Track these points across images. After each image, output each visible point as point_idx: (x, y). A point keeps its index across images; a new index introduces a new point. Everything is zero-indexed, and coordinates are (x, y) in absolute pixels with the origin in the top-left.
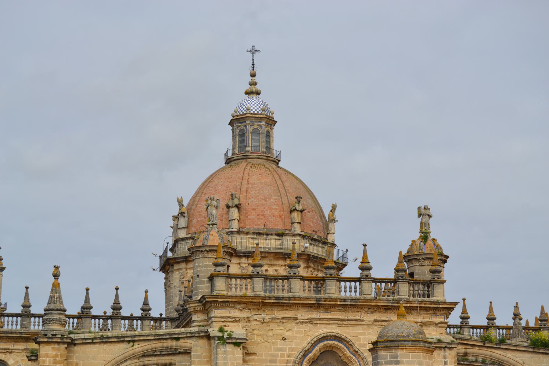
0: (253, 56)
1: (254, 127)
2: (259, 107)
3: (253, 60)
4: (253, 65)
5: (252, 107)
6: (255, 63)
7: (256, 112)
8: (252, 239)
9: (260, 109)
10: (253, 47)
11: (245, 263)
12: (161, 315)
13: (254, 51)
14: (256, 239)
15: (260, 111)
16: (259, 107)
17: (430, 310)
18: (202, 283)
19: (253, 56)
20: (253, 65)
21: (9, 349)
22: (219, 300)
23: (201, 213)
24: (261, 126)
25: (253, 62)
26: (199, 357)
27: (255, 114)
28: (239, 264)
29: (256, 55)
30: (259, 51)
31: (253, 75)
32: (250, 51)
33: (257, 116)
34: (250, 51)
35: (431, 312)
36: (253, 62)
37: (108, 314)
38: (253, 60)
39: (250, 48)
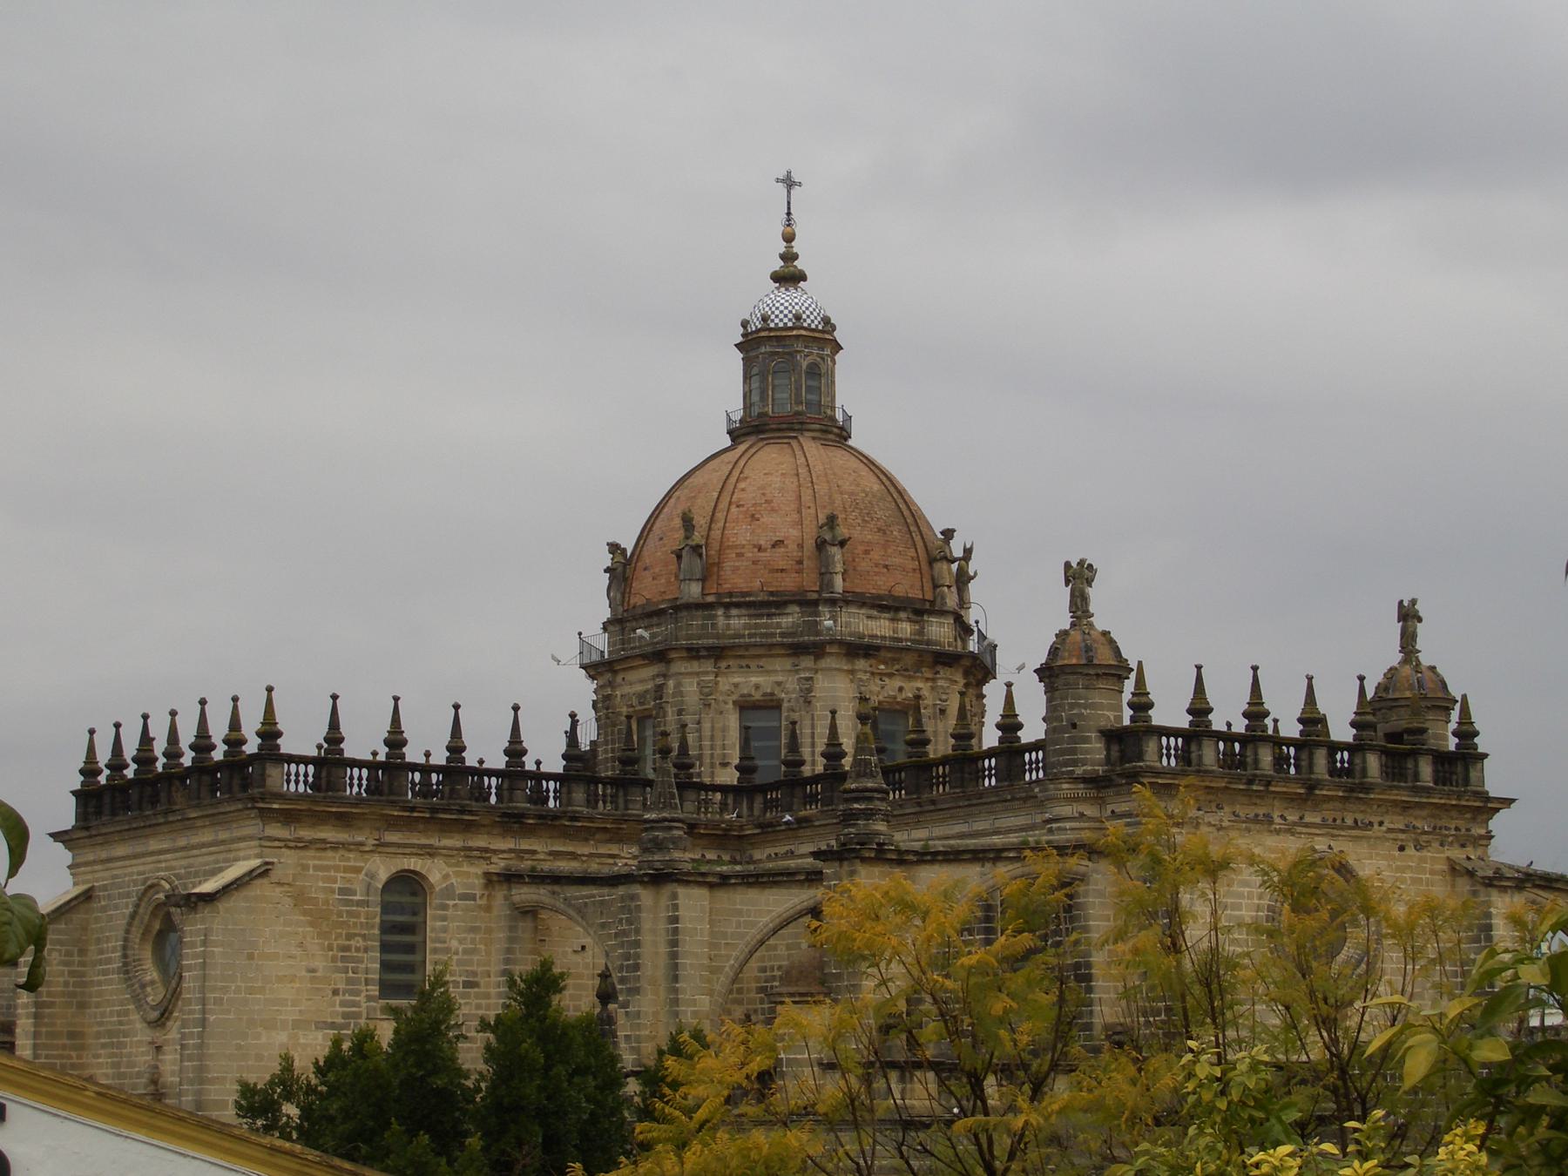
0: (789, 192)
1: (809, 360)
2: (790, 312)
3: (789, 203)
4: (789, 214)
5: (804, 312)
6: (792, 211)
7: (781, 325)
8: (868, 617)
9: (819, 319)
10: (789, 173)
11: (866, 672)
12: (375, 754)
13: (789, 183)
14: (875, 618)
15: (790, 320)
16: (790, 312)
17: (1467, 812)
18: (1086, 740)
19: (789, 192)
20: (789, 214)
21: (430, 846)
22: (1160, 781)
23: (743, 551)
24: (823, 359)
25: (789, 208)
26: (1101, 894)
27: (813, 330)
28: (852, 672)
29: (795, 191)
30: (800, 184)
31: (789, 238)
32: (783, 181)
33: (817, 335)
34: (783, 181)
35: (1468, 816)
36: (789, 208)
37: (434, 761)
38: (789, 203)
39: (782, 175)
